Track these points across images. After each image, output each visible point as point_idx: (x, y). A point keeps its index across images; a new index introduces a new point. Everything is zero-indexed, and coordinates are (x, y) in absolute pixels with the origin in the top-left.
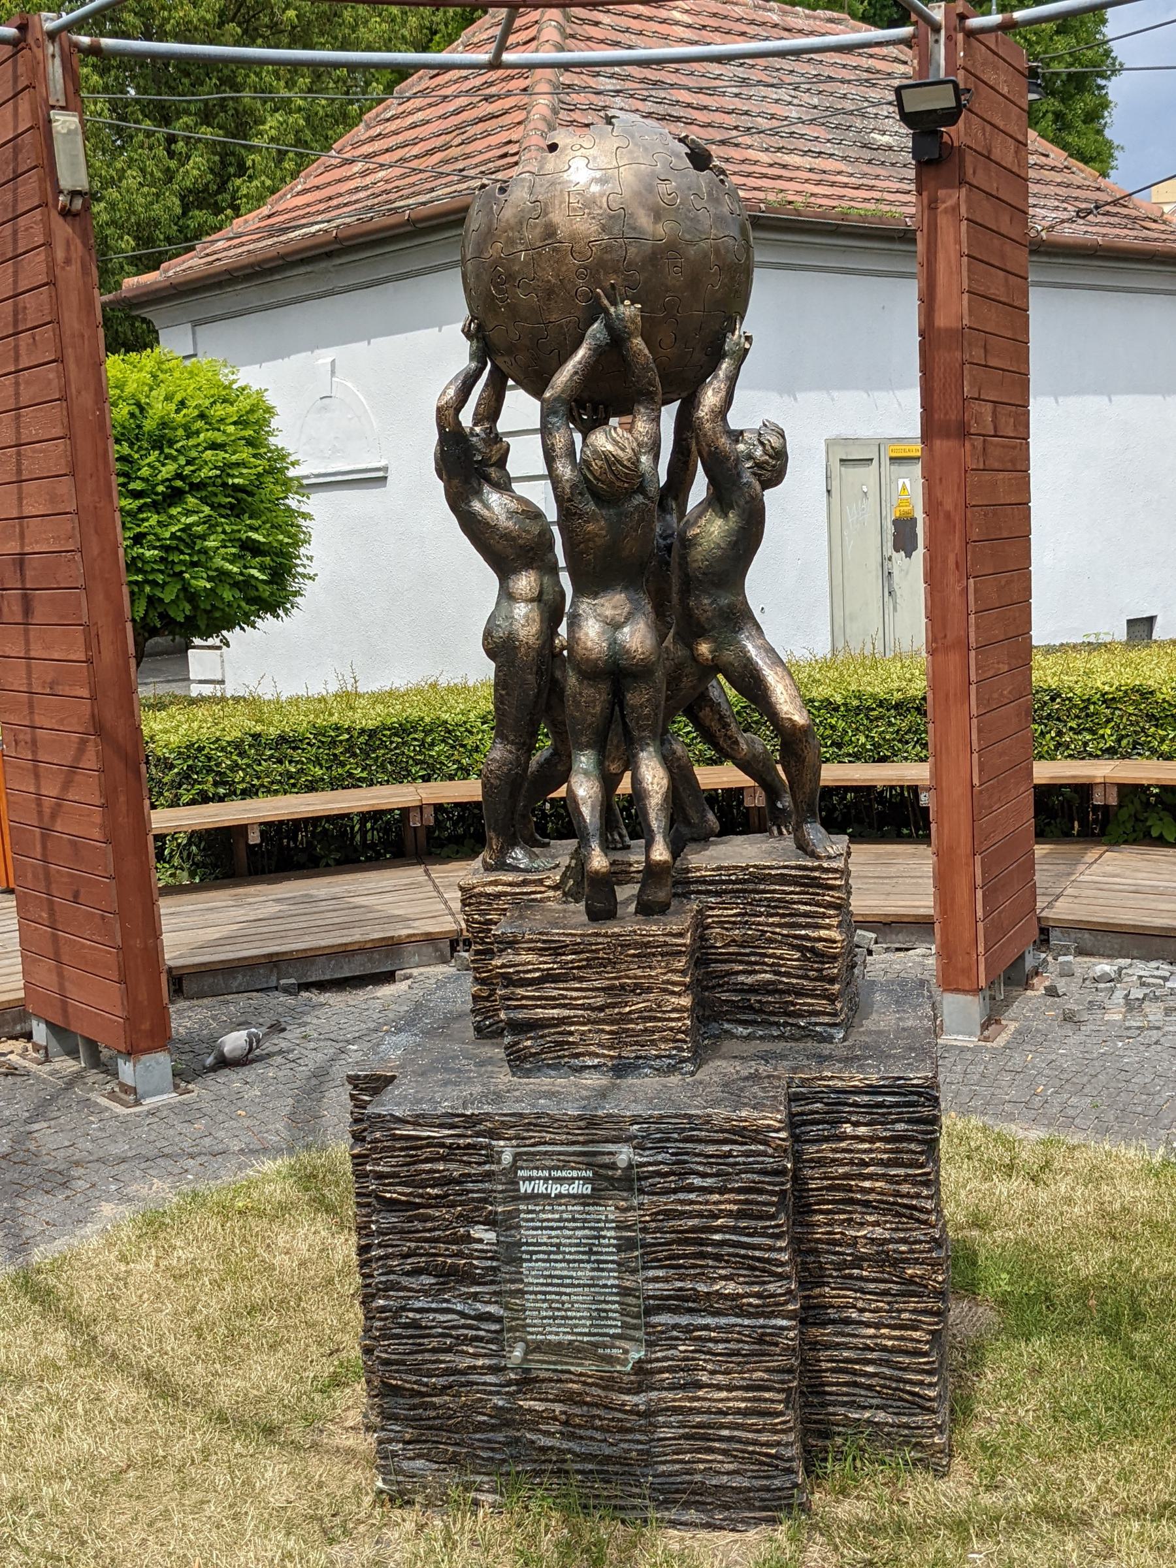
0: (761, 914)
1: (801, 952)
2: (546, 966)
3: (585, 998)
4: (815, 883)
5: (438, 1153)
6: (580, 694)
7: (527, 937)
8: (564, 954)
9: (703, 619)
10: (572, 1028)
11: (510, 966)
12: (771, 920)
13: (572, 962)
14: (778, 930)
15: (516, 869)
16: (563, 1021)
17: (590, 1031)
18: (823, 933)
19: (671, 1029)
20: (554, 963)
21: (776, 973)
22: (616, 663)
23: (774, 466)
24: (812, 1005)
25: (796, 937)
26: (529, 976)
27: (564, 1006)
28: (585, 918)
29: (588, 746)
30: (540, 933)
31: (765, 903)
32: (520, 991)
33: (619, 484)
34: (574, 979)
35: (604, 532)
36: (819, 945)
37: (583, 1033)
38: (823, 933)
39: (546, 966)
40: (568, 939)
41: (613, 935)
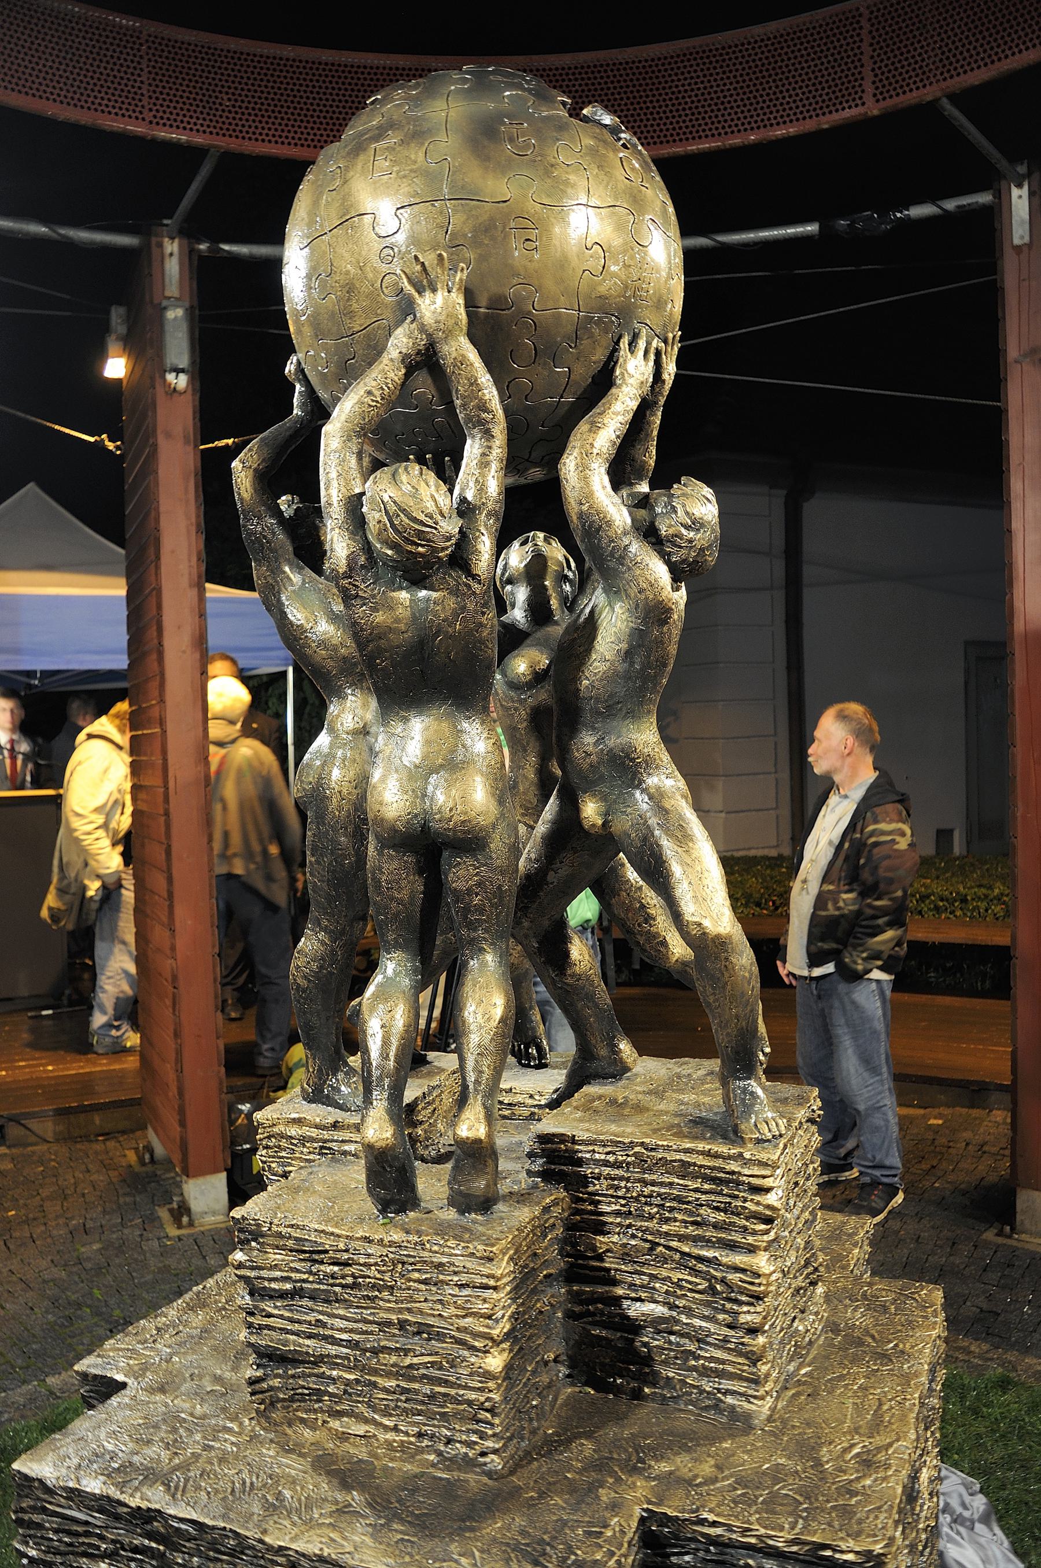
0: (651, 1217)
1: (709, 1280)
2: (298, 1276)
3: (351, 1331)
4: (732, 1180)
5: (98, 1548)
6: (380, 869)
7: (275, 1228)
8: (322, 1262)
9: (585, 766)
10: (335, 1373)
11: (252, 1268)
12: (665, 1228)
13: (333, 1276)
14: (674, 1244)
15: (329, 1101)
16: (320, 1360)
17: (357, 1381)
18: (739, 1259)
19: (470, 1403)
20: (310, 1273)
21: (672, 1307)
22: (425, 828)
23: (690, 541)
24: (723, 1362)
25: (700, 1259)
26: (274, 1285)
27: (325, 1338)
28: (370, 1207)
29: (397, 946)
30: (292, 1226)
31: (658, 1201)
32: (268, 1306)
33: (409, 548)
34: (337, 1301)
35: (402, 627)
36: (734, 1277)
37: (348, 1383)
38: (739, 1259)
39: (298, 1276)
40: (328, 1243)
41: (392, 1244)
